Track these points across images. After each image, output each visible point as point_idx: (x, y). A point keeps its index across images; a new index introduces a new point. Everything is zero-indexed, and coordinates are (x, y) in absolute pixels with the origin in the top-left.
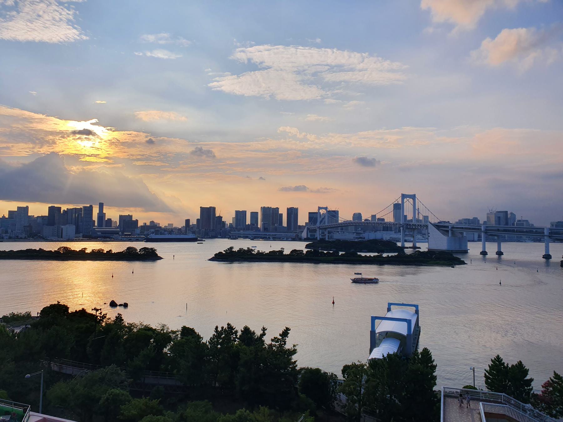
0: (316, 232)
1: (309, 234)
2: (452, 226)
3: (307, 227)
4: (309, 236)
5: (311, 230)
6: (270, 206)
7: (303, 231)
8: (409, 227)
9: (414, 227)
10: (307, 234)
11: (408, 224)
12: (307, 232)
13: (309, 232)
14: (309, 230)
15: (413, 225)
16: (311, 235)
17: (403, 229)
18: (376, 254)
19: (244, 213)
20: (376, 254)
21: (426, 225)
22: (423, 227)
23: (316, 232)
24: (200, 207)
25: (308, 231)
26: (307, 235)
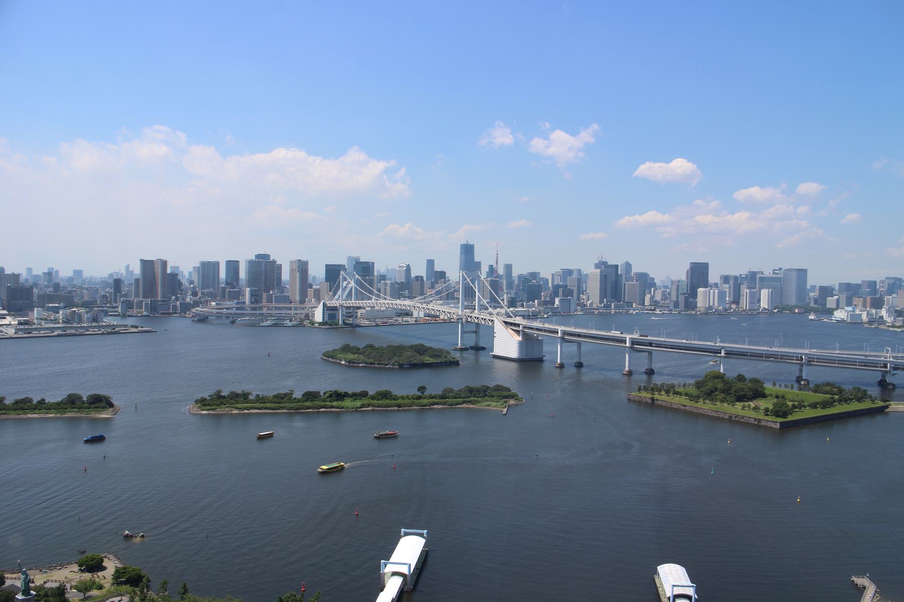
1: (327, 313)
3: (324, 303)
4: (326, 319)
5: (328, 307)
7: (318, 307)
8: (469, 320)
9: (476, 321)
10: (323, 313)
11: (469, 316)
12: (323, 310)
13: (327, 310)
17: (462, 323)
19: (217, 265)
21: (492, 321)
24: (141, 260)
26: (323, 315)
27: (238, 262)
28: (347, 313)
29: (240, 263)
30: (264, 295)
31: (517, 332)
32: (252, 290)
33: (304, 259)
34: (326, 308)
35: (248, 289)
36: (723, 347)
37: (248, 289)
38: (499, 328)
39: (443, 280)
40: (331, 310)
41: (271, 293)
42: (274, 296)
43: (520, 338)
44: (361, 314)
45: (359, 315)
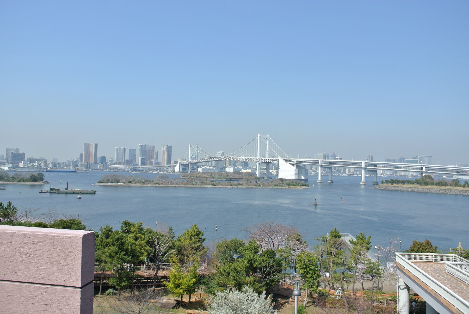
0: (187, 166)
2: (297, 161)
4: (181, 170)
5: (183, 164)
8: (263, 161)
9: (267, 162)
10: (180, 167)
11: (263, 159)
12: (180, 166)
13: (182, 166)
15: (267, 159)
16: (183, 169)
17: (259, 163)
18: (146, 280)
20: (146, 280)
22: (274, 161)
23: (187, 166)
25: (181, 165)
26: (180, 169)
27: (135, 149)
28: (192, 170)
29: (137, 150)
30: (148, 162)
31: (293, 165)
32: (142, 158)
33: (170, 145)
34: (181, 165)
35: (140, 158)
36: (424, 166)
37: (140, 158)
38: (282, 163)
41: (152, 160)
42: (153, 162)
43: (294, 168)
44: (200, 170)
45: (198, 171)
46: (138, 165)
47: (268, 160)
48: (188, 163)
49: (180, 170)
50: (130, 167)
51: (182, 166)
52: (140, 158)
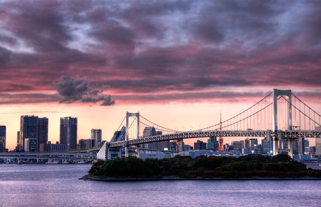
0: (119, 151)
3: (107, 144)
6: (35, 115)
7: (98, 151)
10: (107, 153)
11: (284, 133)
12: (107, 151)
13: (110, 150)
14: (110, 148)
16: (112, 155)
23: (119, 150)
32: (31, 140)
34: (109, 149)
39: (181, 141)
40: (113, 150)
46: (24, 151)
47: (297, 133)
48: (123, 144)
49: (106, 158)
50: (18, 155)
51: (110, 150)
52: (28, 139)
